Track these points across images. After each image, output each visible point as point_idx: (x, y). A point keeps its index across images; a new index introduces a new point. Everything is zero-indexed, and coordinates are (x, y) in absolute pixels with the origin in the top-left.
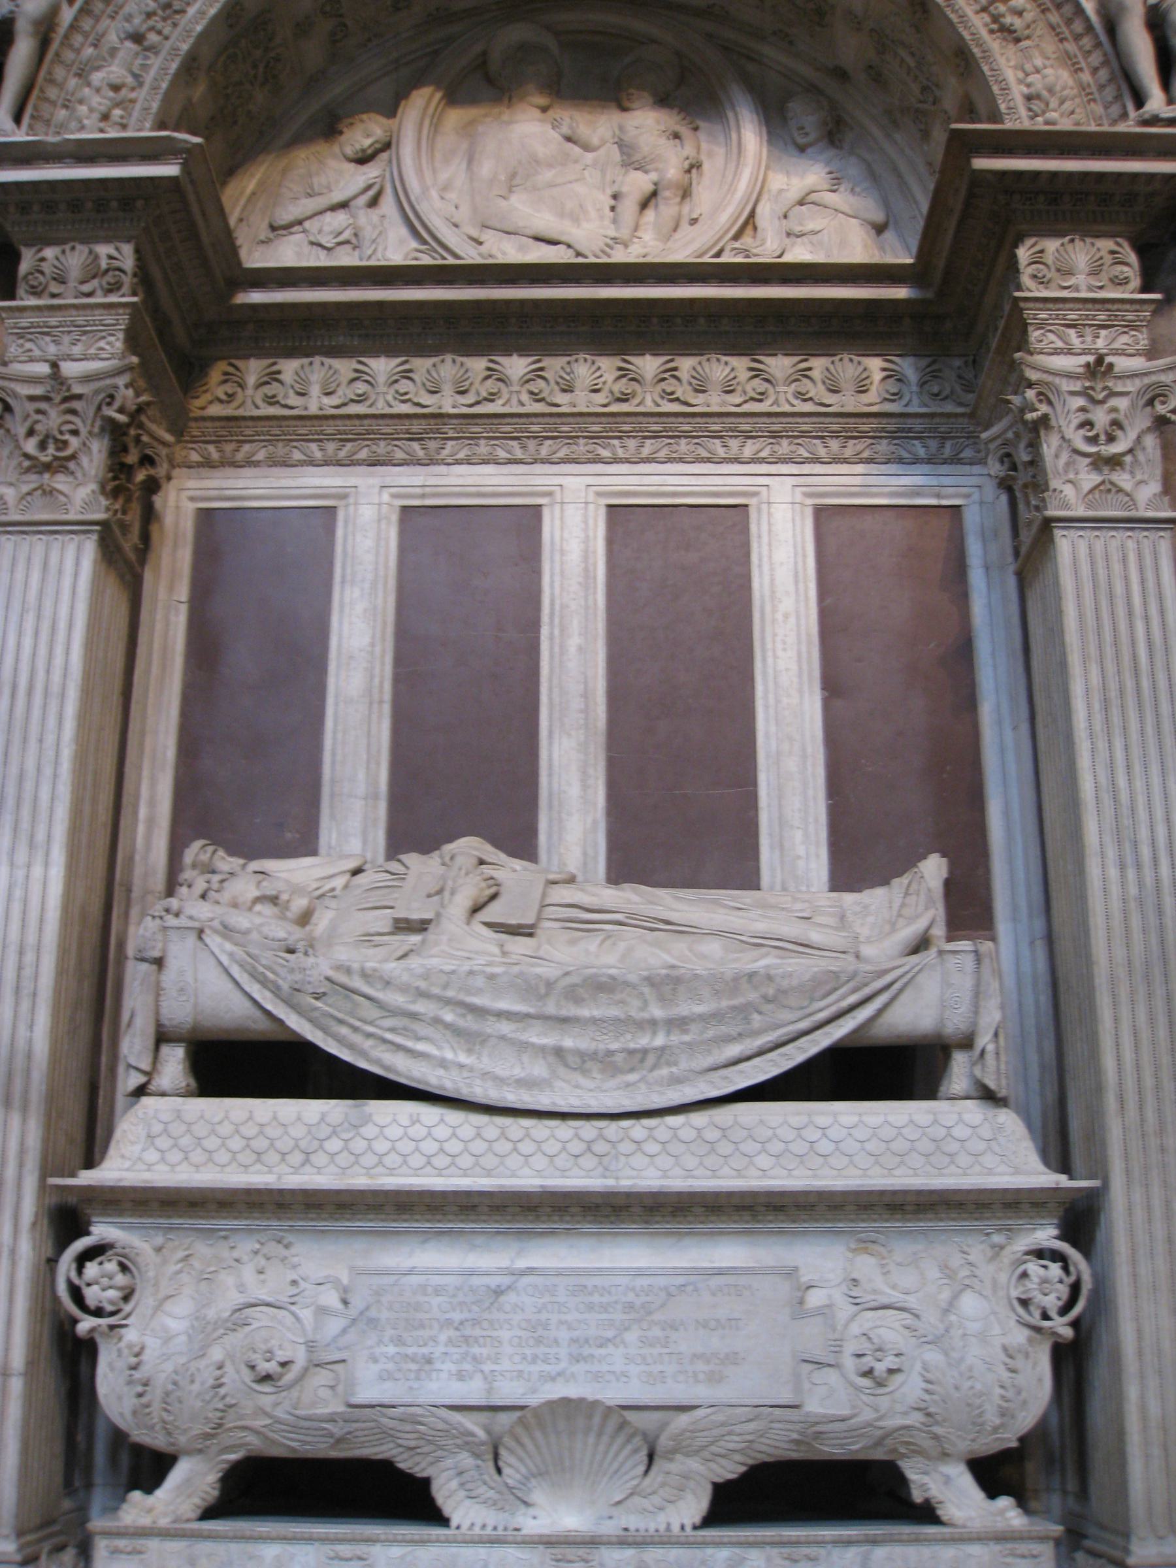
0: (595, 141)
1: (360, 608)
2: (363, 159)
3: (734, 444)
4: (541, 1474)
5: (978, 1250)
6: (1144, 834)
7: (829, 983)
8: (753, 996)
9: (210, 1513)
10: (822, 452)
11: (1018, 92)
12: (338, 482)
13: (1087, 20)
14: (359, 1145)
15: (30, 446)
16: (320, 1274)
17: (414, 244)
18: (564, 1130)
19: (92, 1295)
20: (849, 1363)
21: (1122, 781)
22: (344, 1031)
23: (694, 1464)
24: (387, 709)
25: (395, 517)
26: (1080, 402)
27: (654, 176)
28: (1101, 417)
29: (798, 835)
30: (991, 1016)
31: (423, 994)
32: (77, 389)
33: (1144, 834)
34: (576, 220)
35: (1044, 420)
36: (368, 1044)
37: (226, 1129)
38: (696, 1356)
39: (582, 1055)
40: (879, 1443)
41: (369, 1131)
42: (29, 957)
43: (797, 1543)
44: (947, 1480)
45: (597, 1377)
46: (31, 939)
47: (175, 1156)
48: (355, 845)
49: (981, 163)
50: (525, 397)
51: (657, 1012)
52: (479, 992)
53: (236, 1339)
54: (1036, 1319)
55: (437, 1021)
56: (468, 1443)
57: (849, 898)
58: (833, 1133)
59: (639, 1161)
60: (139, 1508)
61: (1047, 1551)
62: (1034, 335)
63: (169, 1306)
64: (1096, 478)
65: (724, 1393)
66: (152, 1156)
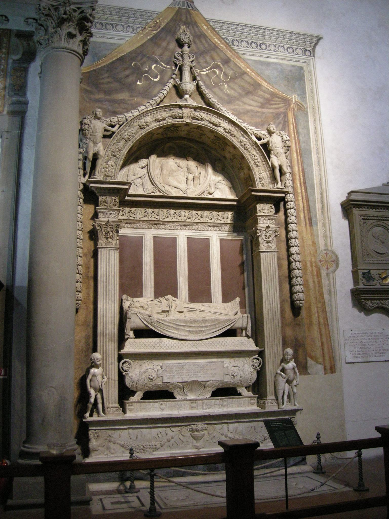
0: (183, 167)
1: (148, 254)
2: (142, 168)
3: (207, 227)
4: (188, 391)
5: (247, 359)
6: (271, 300)
7: (227, 320)
8: (217, 322)
9: (142, 399)
10: (221, 229)
11: (258, 176)
12: (143, 232)
13: (269, 166)
14: (161, 345)
15: (104, 233)
16: (157, 364)
17: (152, 186)
18: (190, 342)
19: (125, 369)
20: (230, 374)
21: (268, 292)
22: (159, 328)
23: (210, 389)
24: (153, 272)
25: (152, 238)
26: (265, 232)
27: (193, 175)
28: (268, 235)
29: (217, 294)
30: (249, 325)
31: (171, 323)
32: (111, 224)
33: (271, 300)
34: (180, 183)
35: (260, 236)
36: (162, 330)
37: (142, 343)
38: (210, 374)
39: (193, 331)
40: (234, 385)
41: (163, 343)
42: (113, 319)
43: (223, 399)
44: (243, 390)
45: (197, 377)
46: (113, 316)
47: (135, 348)
48: (149, 296)
49: (253, 193)
50: (173, 217)
51: (203, 325)
52: (178, 322)
53: (147, 374)
54: (255, 368)
55: (172, 327)
56: (180, 387)
57: (225, 304)
58: (228, 342)
59: (201, 346)
60: (132, 399)
61: (256, 399)
62: (259, 220)
63: (135, 370)
64: (267, 244)
65: (214, 379)
66: (131, 348)
